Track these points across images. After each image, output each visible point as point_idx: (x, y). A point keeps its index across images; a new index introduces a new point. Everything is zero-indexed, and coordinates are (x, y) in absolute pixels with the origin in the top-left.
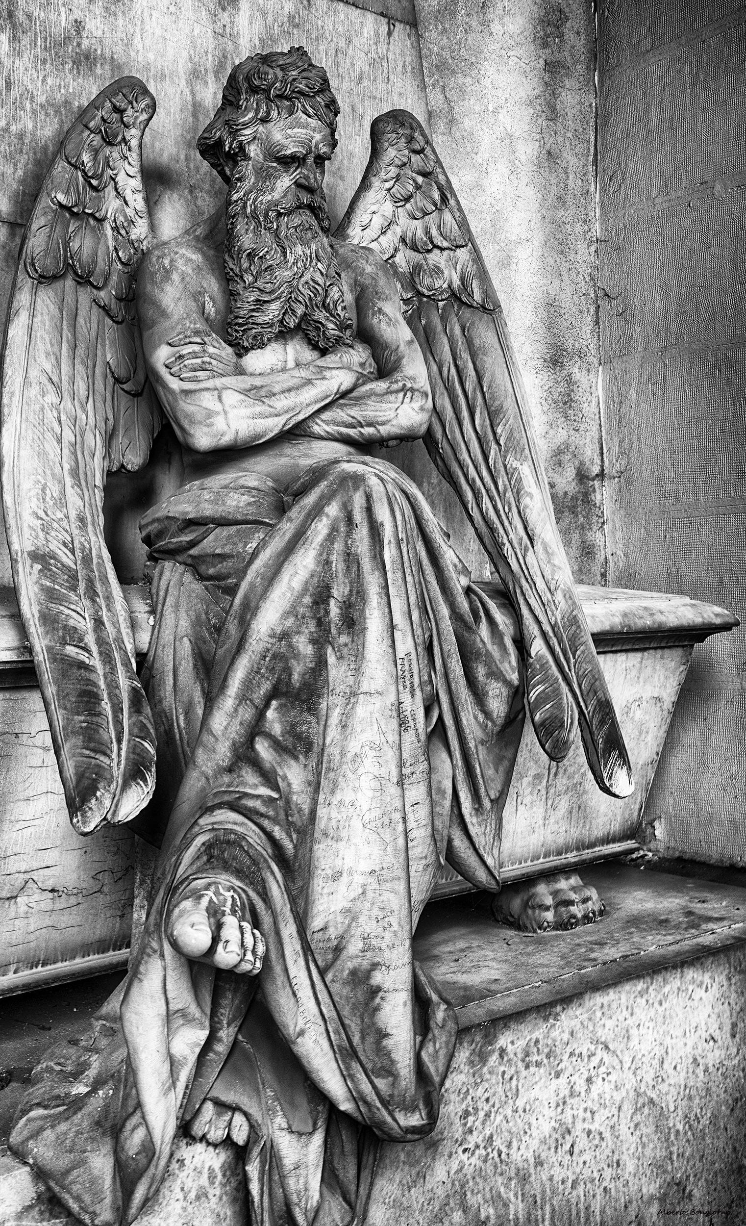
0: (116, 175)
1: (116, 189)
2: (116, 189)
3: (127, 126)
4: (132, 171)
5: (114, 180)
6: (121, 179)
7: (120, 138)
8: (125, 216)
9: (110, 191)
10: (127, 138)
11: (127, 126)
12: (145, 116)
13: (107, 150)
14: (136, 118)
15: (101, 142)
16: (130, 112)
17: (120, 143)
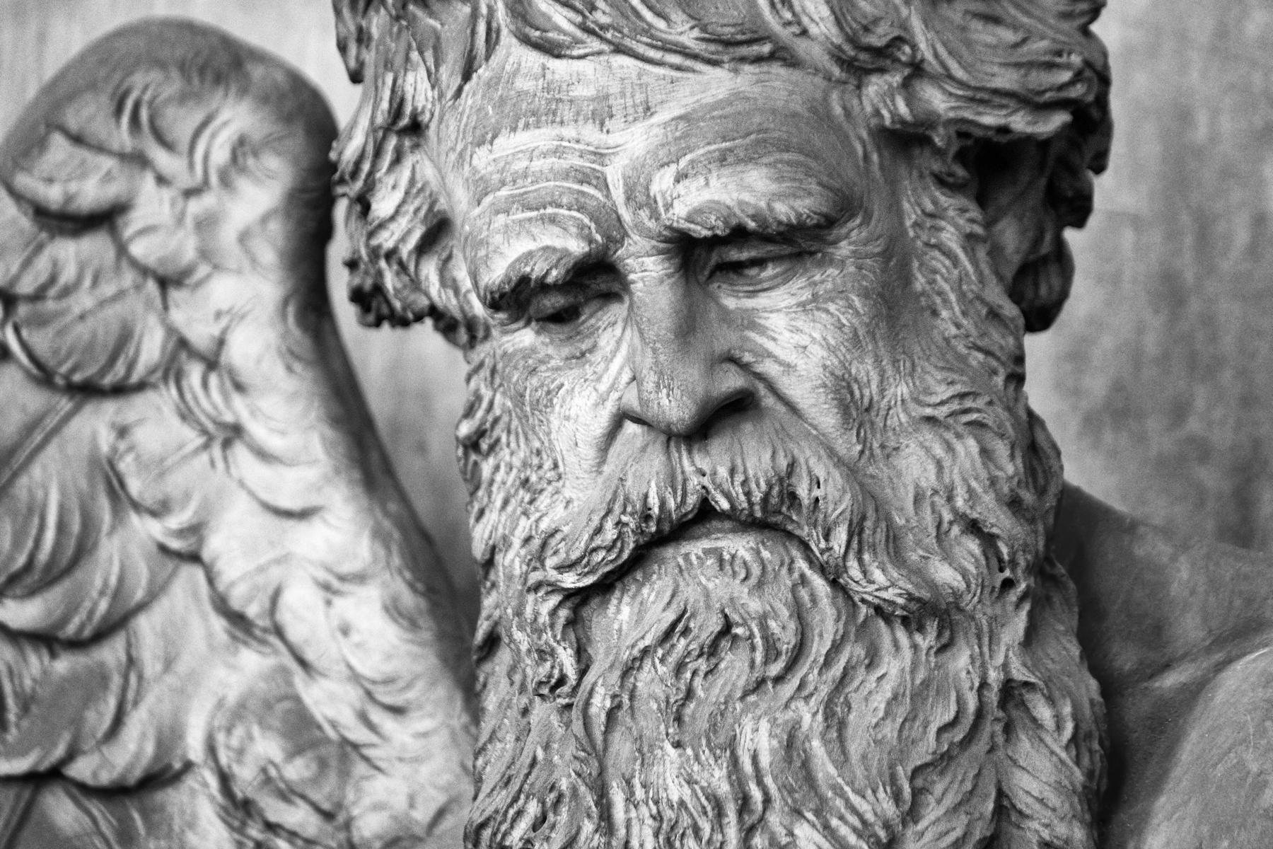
0: (195, 530)
1: (222, 605)
2: (222, 605)
3: (168, 281)
4: (289, 487)
5: (194, 557)
6: (235, 547)
7: (151, 348)
8: (301, 730)
9: (180, 616)
10: (200, 333)
11: (168, 281)
12: (259, 199)
13: (95, 425)
14: (206, 225)
15: (34, 399)
16: (151, 206)
17: (171, 371)
